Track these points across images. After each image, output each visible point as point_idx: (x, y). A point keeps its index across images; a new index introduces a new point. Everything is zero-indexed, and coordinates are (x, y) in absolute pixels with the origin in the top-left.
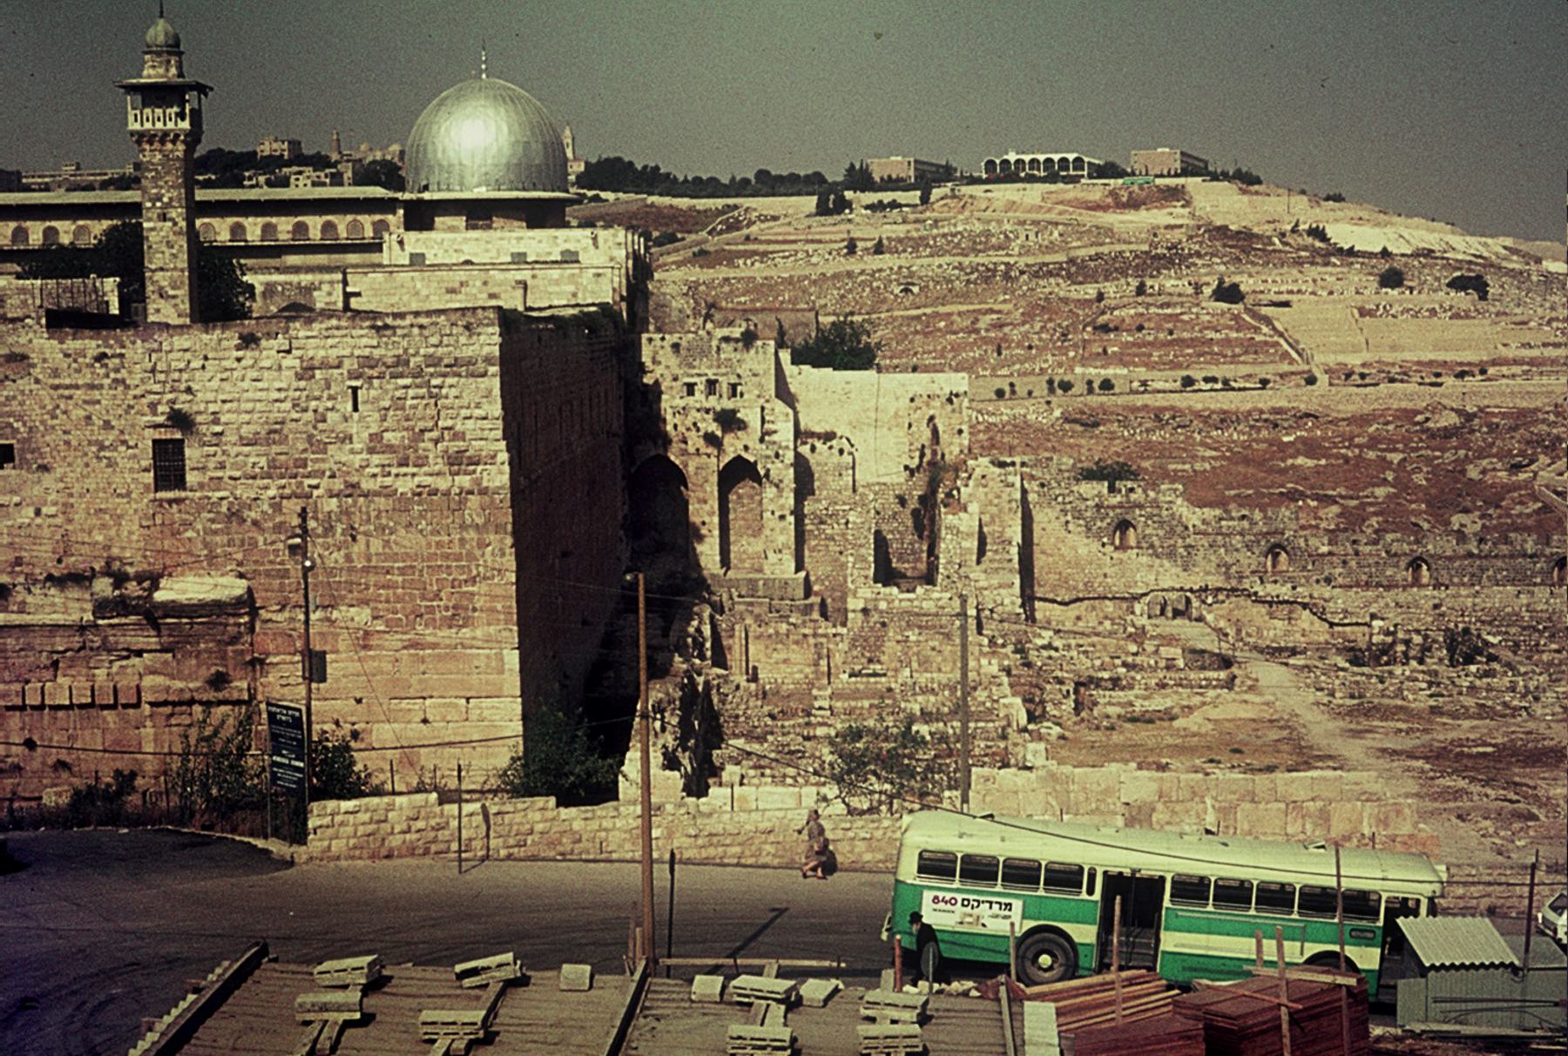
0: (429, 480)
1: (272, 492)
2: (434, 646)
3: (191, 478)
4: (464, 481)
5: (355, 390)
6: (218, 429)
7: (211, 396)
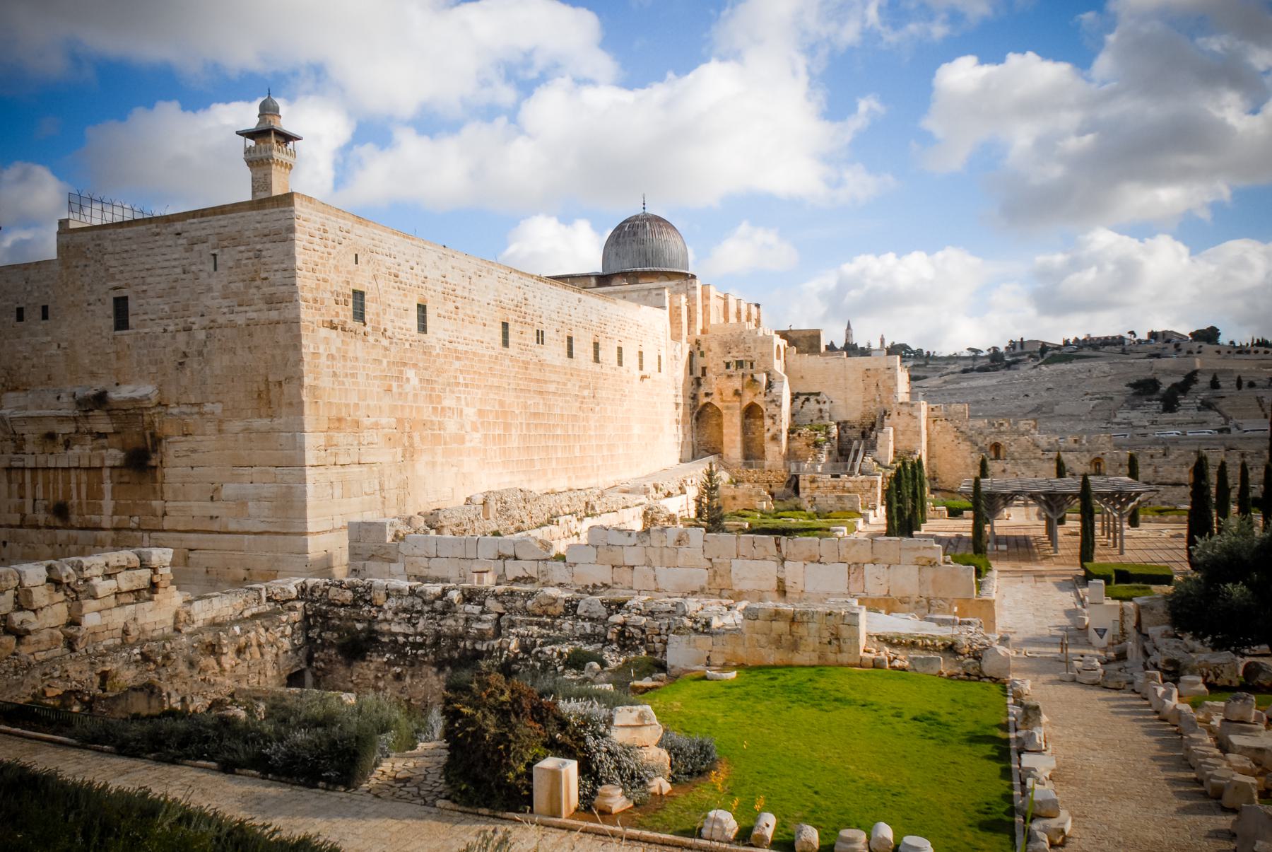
0: (254, 315)
1: (171, 328)
2: (258, 432)
3: (132, 321)
4: (274, 315)
5: (214, 255)
6: (145, 288)
7: (141, 267)
